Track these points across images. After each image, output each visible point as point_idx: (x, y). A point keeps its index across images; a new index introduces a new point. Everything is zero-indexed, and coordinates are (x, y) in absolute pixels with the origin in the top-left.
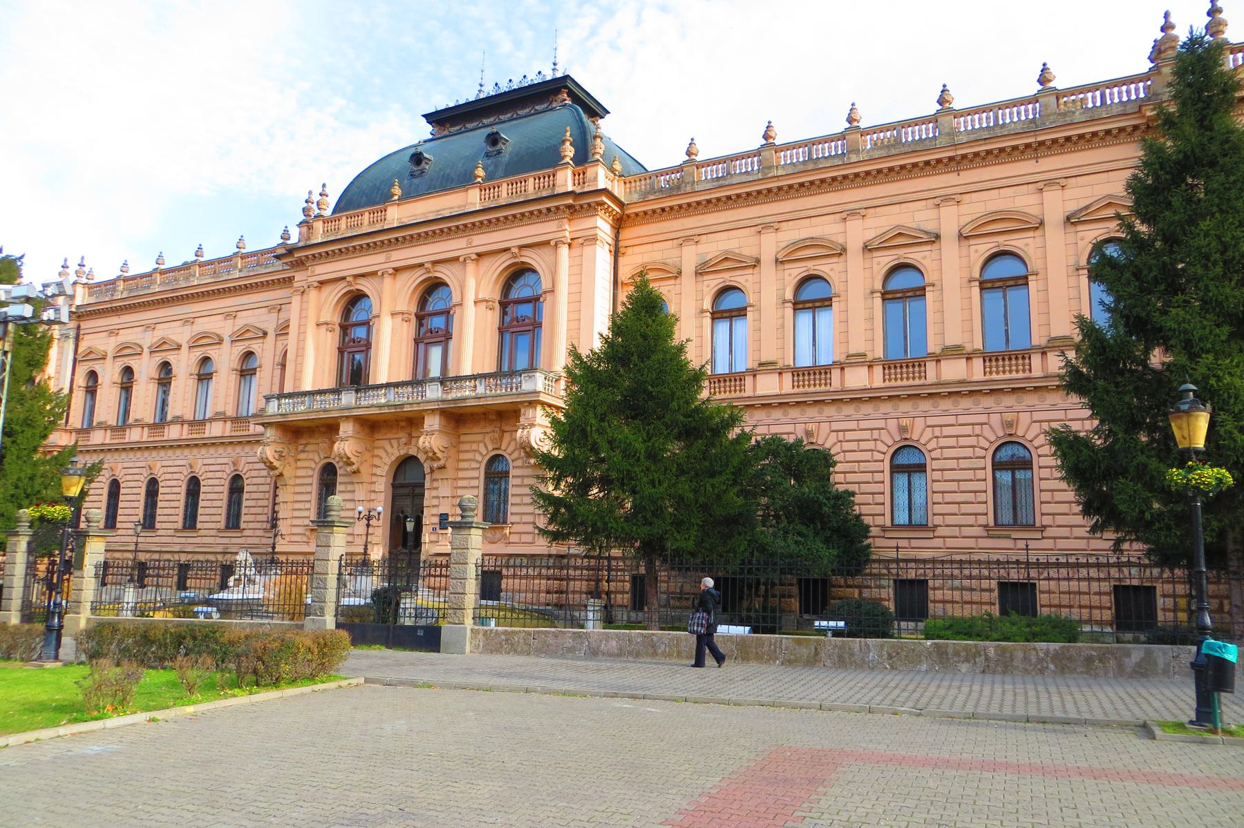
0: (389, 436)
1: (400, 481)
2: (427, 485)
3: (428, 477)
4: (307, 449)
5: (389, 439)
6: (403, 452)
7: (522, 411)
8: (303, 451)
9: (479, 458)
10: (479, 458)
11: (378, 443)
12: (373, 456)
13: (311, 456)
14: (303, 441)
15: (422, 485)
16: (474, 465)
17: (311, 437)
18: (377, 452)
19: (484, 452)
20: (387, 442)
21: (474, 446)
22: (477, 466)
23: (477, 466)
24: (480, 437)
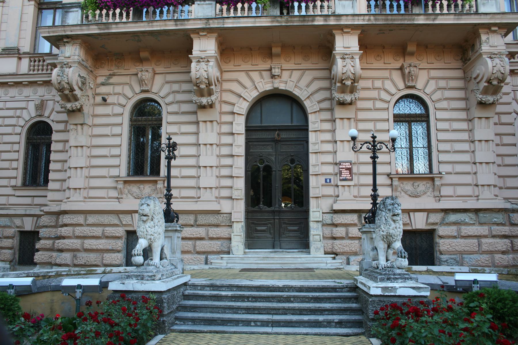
0: (244, 67)
1: (256, 123)
2: (311, 127)
3: (311, 118)
4: (111, 81)
5: (247, 72)
6: (268, 87)
7: (484, 37)
8: (103, 84)
9: (384, 96)
10: (387, 97)
11: (226, 76)
12: (222, 91)
13: (118, 89)
14: (105, 72)
15: (305, 129)
16: (379, 105)
17: (118, 68)
18: (226, 86)
19: (393, 90)
20: (243, 74)
21: (378, 84)
22: (385, 106)
23: (385, 106)
24: (386, 73)
